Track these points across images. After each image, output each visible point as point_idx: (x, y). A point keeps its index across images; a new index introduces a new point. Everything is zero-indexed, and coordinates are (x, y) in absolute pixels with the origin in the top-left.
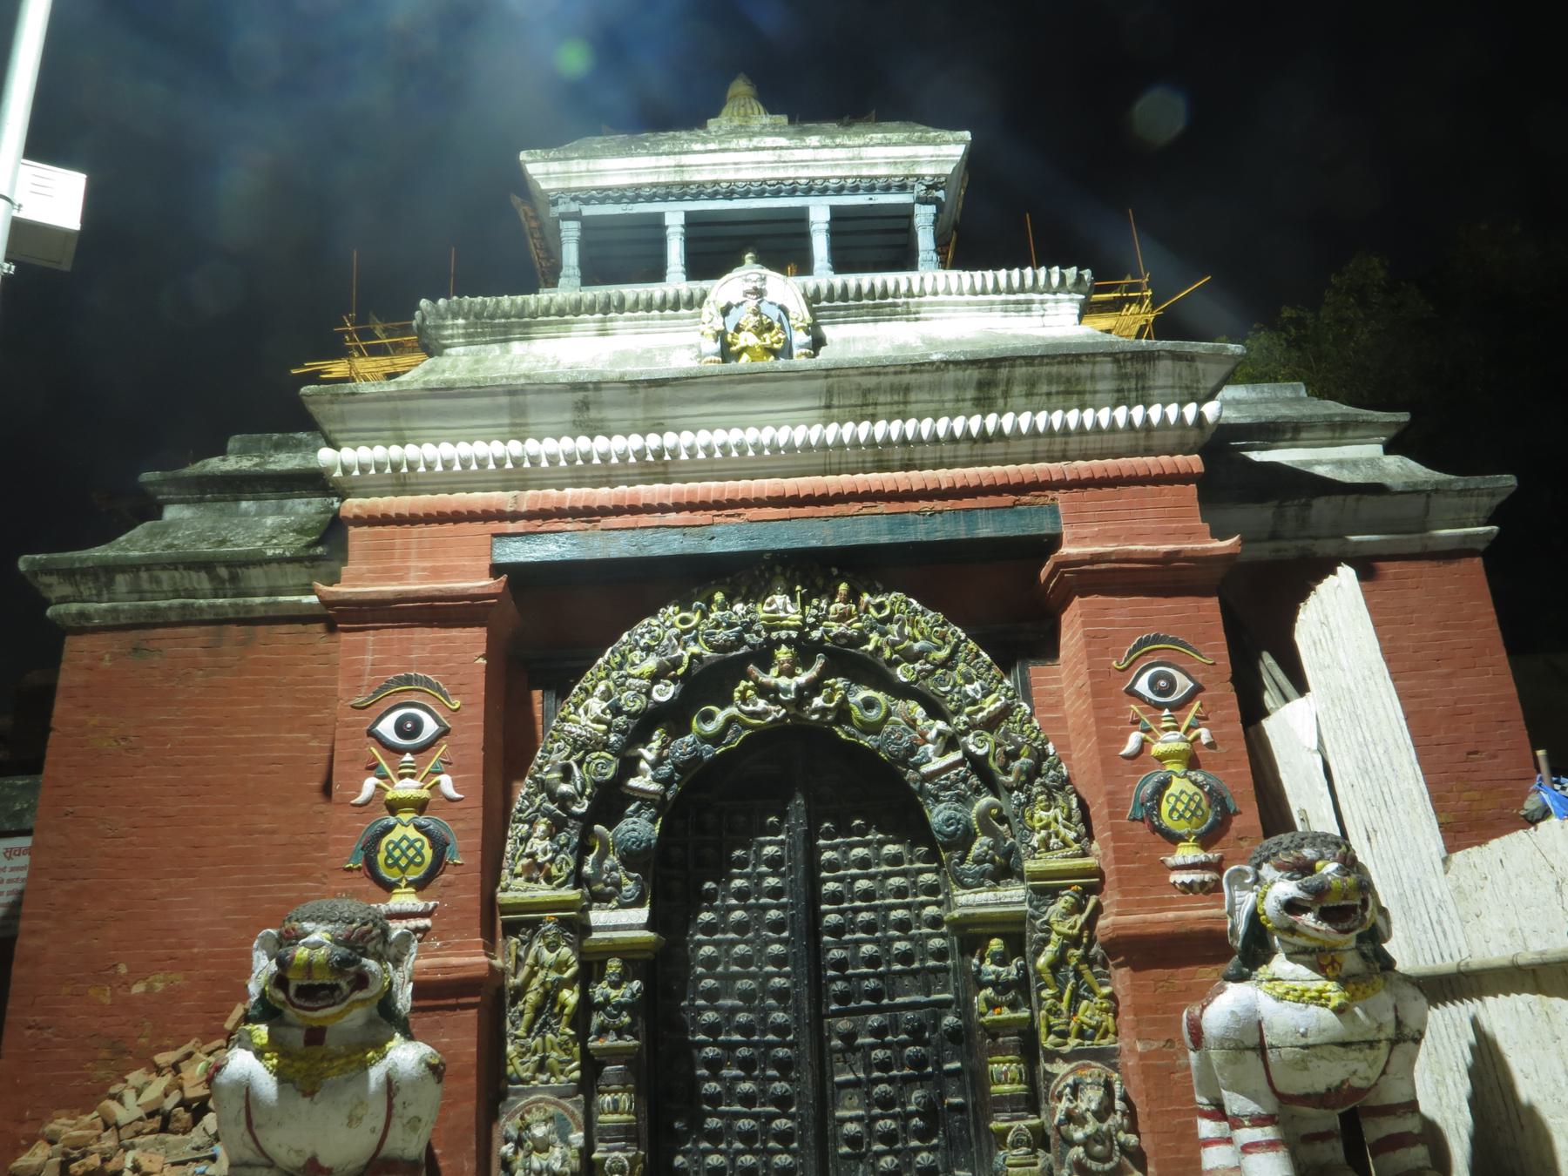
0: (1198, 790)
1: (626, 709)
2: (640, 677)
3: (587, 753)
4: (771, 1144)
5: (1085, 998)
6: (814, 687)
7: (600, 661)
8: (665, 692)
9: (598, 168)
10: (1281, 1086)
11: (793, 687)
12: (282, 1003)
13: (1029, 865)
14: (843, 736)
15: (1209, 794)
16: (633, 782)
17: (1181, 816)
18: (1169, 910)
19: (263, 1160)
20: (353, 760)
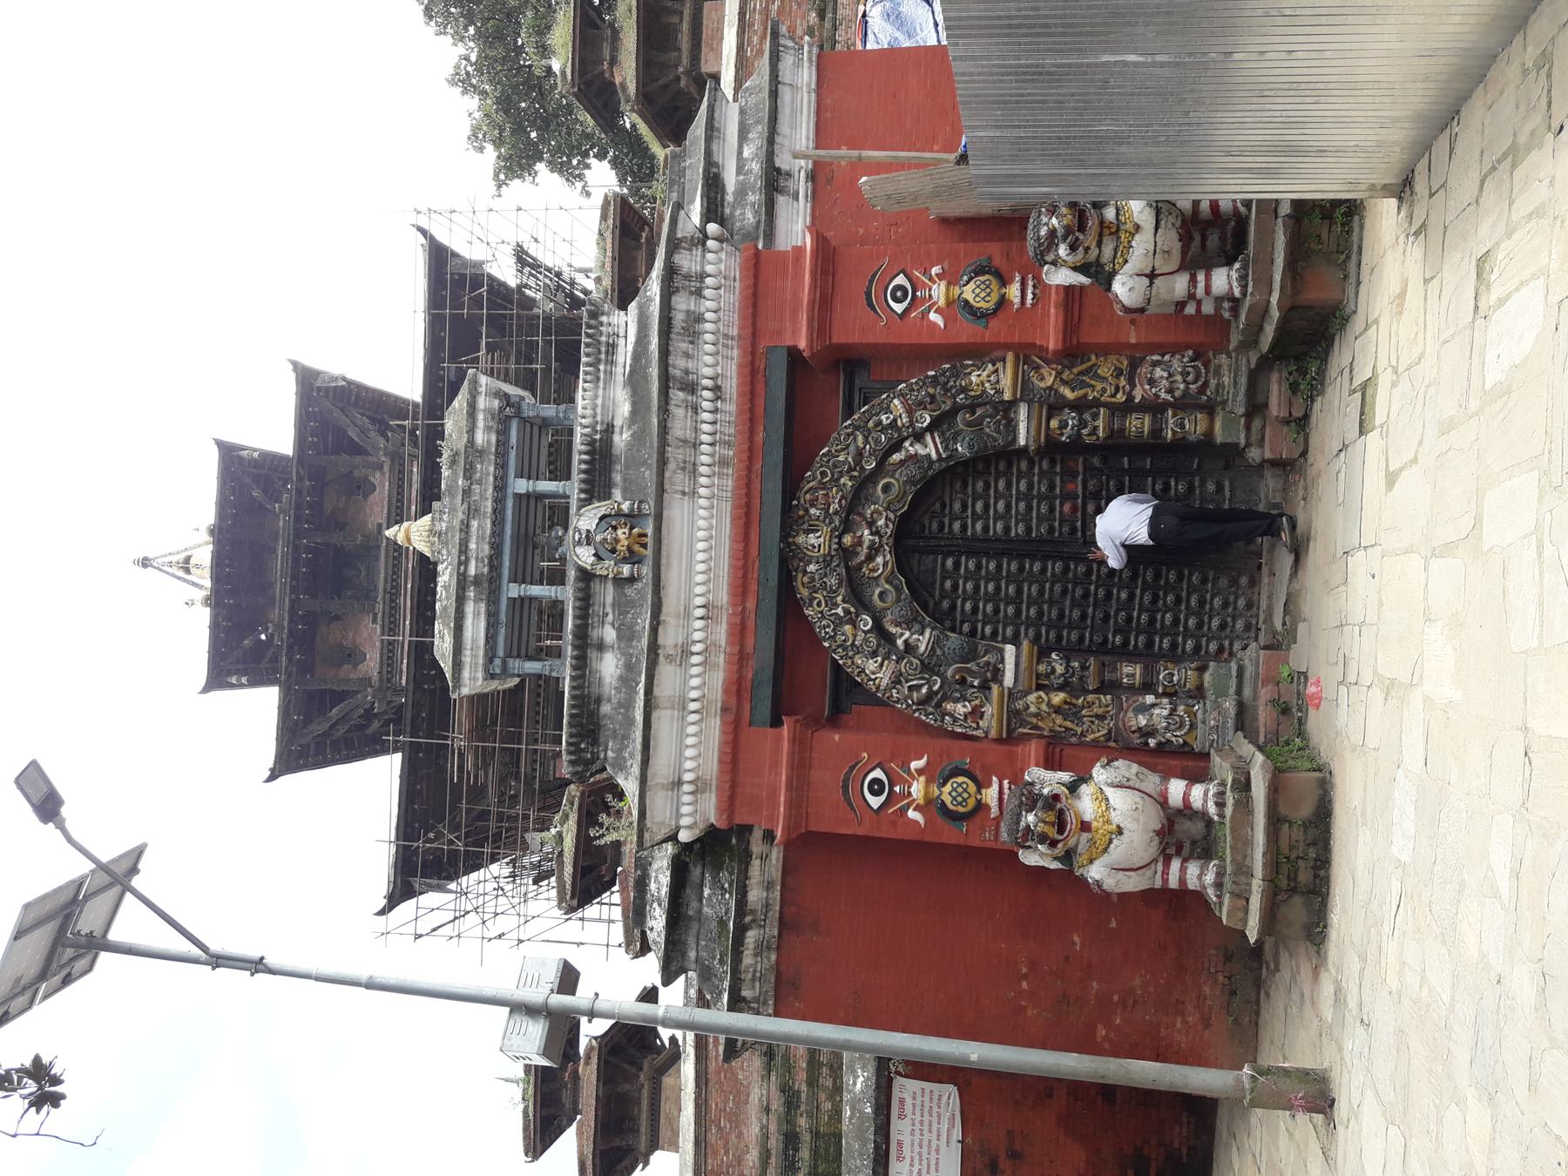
0: (972, 282)
1: (875, 648)
2: (855, 636)
3: (901, 675)
4: (1162, 582)
5: (1096, 371)
6: (871, 524)
7: (841, 662)
8: (867, 622)
9: (470, 638)
11: (870, 537)
13: (1007, 396)
14: (906, 508)
15: (977, 274)
16: (922, 648)
17: (989, 295)
18: (1049, 311)
19: (1153, 865)
20: (894, 824)
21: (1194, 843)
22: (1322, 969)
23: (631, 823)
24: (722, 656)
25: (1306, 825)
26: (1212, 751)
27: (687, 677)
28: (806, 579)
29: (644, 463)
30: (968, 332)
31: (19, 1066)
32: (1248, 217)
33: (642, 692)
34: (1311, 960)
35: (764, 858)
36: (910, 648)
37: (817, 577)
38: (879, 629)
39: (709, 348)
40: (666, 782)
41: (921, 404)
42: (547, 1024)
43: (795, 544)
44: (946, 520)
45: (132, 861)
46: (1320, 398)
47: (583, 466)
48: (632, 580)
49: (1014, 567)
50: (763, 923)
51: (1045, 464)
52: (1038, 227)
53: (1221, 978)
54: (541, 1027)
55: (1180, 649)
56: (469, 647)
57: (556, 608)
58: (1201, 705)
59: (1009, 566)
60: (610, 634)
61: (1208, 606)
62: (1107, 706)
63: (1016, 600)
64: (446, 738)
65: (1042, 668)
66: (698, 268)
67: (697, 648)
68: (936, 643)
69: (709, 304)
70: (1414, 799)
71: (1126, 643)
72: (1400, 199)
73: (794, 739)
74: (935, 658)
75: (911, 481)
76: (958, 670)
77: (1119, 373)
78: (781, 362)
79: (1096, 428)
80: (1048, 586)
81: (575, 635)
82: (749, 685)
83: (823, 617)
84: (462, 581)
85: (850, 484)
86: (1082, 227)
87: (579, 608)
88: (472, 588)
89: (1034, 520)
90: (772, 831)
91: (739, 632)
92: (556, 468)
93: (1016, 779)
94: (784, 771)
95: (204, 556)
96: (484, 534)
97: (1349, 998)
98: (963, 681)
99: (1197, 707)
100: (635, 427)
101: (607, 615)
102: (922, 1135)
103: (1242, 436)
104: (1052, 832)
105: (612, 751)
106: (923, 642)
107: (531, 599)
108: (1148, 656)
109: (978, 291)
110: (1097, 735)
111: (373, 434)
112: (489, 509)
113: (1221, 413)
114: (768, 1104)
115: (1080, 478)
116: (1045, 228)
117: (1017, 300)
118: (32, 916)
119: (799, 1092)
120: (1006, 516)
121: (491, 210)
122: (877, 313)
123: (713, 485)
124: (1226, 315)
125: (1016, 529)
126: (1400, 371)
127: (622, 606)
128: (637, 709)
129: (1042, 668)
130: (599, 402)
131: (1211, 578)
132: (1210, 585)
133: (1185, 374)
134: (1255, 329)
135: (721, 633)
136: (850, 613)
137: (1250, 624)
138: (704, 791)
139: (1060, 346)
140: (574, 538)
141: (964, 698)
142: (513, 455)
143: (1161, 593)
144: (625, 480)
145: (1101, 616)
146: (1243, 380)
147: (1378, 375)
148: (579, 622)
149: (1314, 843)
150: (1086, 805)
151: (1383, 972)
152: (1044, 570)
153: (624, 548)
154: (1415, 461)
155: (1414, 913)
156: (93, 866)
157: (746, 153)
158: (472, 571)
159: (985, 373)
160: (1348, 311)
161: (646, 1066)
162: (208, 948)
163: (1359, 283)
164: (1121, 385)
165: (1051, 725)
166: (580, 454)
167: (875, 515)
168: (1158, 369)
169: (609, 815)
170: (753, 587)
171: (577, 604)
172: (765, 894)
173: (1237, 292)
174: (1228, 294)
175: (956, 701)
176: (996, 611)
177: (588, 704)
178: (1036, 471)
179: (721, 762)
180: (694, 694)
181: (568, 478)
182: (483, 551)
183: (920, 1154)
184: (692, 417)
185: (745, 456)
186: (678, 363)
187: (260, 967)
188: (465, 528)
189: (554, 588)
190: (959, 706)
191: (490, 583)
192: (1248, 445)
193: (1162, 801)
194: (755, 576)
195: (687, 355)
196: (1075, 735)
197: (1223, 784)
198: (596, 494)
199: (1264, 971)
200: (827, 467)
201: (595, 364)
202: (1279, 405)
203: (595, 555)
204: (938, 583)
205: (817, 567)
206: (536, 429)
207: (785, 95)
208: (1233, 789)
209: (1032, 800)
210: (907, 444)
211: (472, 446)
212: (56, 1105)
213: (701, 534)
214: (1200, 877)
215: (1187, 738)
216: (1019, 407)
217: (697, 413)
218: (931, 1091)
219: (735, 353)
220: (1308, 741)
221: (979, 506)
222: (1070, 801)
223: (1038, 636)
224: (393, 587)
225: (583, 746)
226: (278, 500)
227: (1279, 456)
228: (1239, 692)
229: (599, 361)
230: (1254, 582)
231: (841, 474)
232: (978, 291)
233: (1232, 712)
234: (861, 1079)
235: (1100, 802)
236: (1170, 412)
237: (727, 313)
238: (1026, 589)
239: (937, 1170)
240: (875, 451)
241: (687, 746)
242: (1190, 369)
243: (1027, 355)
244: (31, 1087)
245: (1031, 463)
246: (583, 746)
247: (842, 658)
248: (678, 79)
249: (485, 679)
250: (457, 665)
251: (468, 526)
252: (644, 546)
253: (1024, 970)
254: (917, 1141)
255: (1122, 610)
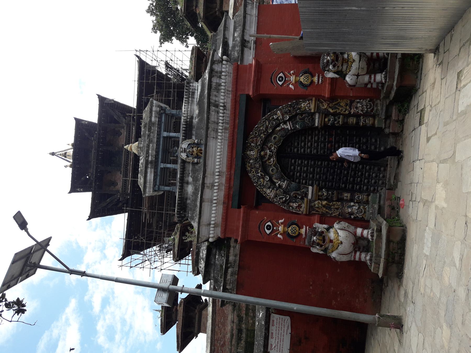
2: (264, 182)
3: (277, 194)
4: (357, 169)
6: (270, 149)
7: (259, 190)
8: (267, 178)
9: (149, 179)
10: (365, 73)
12: (325, 247)
13: (312, 111)
15: (304, 74)
16: (284, 186)
21: (364, 247)
22: (401, 286)
23: (195, 236)
24: (224, 187)
25: (398, 243)
26: (370, 220)
27: (213, 193)
28: (249, 165)
29: (202, 128)
30: (301, 91)
31: (13, 301)
32: (388, 59)
33: (199, 197)
34: (398, 283)
35: (234, 247)
36: (280, 186)
37: (253, 164)
38: (271, 180)
39: (222, 94)
40: (206, 224)
41: (286, 113)
42: (169, 294)
43: (246, 154)
44: (293, 148)
45: (47, 242)
46: (407, 114)
47: (184, 129)
48: (197, 163)
49: (312, 163)
50: (233, 266)
51: (323, 132)
52: (323, 60)
53: (370, 288)
54: (167, 295)
55: (362, 189)
56: (148, 182)
57: (175, 171)
58: (368, 206)
59: (311, 162)
60: (190, 179)
61: (371, 176)
62: (339, 205)
63: (313, 173)
64: (141, 209)
65: (320, 193)
66: (220, 70)
67: (216, 184)
68: (288, 185)
69: (223, 81)
70: (431, 236)
71: (346, 186)
72: (435, 54)
73: (244, 212)
74: (288, 190)
75: (282, 136)
76: (295, 193)
77: (347, 105)
78: (244, 98)
79: (339, 121)
80: (322, 169)
81: (180, 179)
82: (231, 196)
83: (254, 176)
84: (147, 162)
85: (264, 136)
86: (337, 60)
87: (181, 171)
88: (150, 164)
89: (319, 149)
90: (237, 239)
91: (229, 180)
92: (176, 129)
93: (311, 227)
94: (241, 222)
95: (71, 152)
96: (154, 148)
97: (409, 295)
98: (296, 197)
99: (366, 207)
100: (200, 117)
101: (190, 173)
102: (279, 331)
103: (384, 125)
104: (321, 243)
105: (190, 214)
106: (284, 185)
107: (167, 168)
108: (352, 191)
109: (305, 79)
110: (336, 214)
111: (122, 118)
112: (155, 141)
113: (377, 118)
114: (233, 320)
115: (333, 137)
116: (326, 60)
117: (316, 82)
118: (18, 257)
119: (243, 317)
120: (310, 147)
121: (158, 51)
122: (274, 84)
123: (223, 135)
124: (380, 88)
125: (314, 152)
126: (433, 106)
127: (194, 171)
128: (198, 202)
129: (320, 193)
130: (189, 109)
131: (372, 168)
132: (372, 170)
133: (367, 106)
134: (389, 92)
135: (224, 180)
136: (263, 175)
137: (384, 182)
138: (217, 227)
139: (329, 96)
140: (180, 150)
141: (296, 202)
142: (163, 125)
143: (357, 172)
144: (196, 133)
145: (338, 178)
146: (384, 108)
147: (426, 108)
148: (181, 175)
149: (400, 249)
150: (332, 235)
151: (419, 287)
152: (322, 164)
153: (195, 154)
154: (436, 134)
155: (429, 270)
156: (36, 243)
157: (236, 35)
158: (150, 159)
159: (306, 104)
160: (417, 88)
161: (197, 308)
162: (69, 268)
163: (421, 79)
164: (347, 109)
165: (322, 210)
166: (183, 125)
167: (271, 146)
168: (359, 104)
169: (189, 233)
170: (234, 167)
171: (181, 170)
172: (234, 258)
173: (383, 81)
174: (381, 82)
175: (293, 203)
176: (307, 176)
177: (183, 199)
178: (320, 134)
179: (222, 218)
180: (215, 198)
181: (179, 132)
182: (153, 153)
183: (278, 337)
184: (217, 115)
185: (232, 127)
186: (213, 98)
187: (84, 274)
188: (148, 146)
189: (174, 165)
190: (294, 204)
191: (155, 163)
192: (385, 128)
193: (355, 234)
194: (234, 163)
195: (216, 96)
196: (329, 214)
197: (373, 230)
198: (187, 137)
199: (384, 286)
200: (257, 131)
201: (188, 98)
202: (395, 116)
203: (186, 156)
204: (289, 167)
205: (253, 161)
206: (170, 117)
207: (248, 17)
208: (376, 231)
209: (315, 233)
210: (281, 125)
211: (151, 122)
212: (23, 313)
213: (218, 150)
214: (365, 257)
215: (363, 216)
216: (316, 115)
217: (218, 114)
218: (282, 318)
219: (230, 95)
220: (400, 218)
221: (303, 144)
222: (327, 233)
223: (319, 184)
224: (126, 163)
225: (181, 212)
226: (93, 136)
227: (394, 132)
228: (379, 202)
229: (189, 97)
230: (385, 170)
231: (261, 133)
232: (305, 79)
233: (377, 209)
234: (261, 314)
235: (336, 234)
236: (362, 117)
237: (228, 83)
238: (316, 169)
239: (283, 342)
240: (272, 126)
241: (213, 213)
242: (368, 104)
243: (319, 98)
244: (16, 307)
245: (319, 132)
246: (181, 212)
247: (259, 189)
248: (216, 12)
249: (153, 192)
250: (145, 187)
251: (149, 146)
252: (201, 153)
253: (311, 283)
254: (277, 333)
255: (345, 177)
